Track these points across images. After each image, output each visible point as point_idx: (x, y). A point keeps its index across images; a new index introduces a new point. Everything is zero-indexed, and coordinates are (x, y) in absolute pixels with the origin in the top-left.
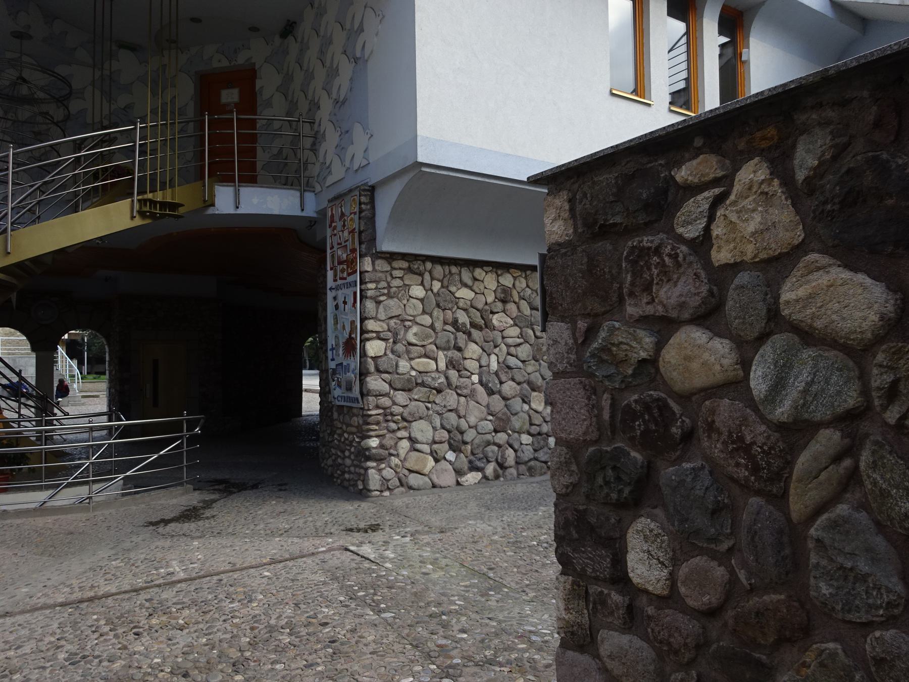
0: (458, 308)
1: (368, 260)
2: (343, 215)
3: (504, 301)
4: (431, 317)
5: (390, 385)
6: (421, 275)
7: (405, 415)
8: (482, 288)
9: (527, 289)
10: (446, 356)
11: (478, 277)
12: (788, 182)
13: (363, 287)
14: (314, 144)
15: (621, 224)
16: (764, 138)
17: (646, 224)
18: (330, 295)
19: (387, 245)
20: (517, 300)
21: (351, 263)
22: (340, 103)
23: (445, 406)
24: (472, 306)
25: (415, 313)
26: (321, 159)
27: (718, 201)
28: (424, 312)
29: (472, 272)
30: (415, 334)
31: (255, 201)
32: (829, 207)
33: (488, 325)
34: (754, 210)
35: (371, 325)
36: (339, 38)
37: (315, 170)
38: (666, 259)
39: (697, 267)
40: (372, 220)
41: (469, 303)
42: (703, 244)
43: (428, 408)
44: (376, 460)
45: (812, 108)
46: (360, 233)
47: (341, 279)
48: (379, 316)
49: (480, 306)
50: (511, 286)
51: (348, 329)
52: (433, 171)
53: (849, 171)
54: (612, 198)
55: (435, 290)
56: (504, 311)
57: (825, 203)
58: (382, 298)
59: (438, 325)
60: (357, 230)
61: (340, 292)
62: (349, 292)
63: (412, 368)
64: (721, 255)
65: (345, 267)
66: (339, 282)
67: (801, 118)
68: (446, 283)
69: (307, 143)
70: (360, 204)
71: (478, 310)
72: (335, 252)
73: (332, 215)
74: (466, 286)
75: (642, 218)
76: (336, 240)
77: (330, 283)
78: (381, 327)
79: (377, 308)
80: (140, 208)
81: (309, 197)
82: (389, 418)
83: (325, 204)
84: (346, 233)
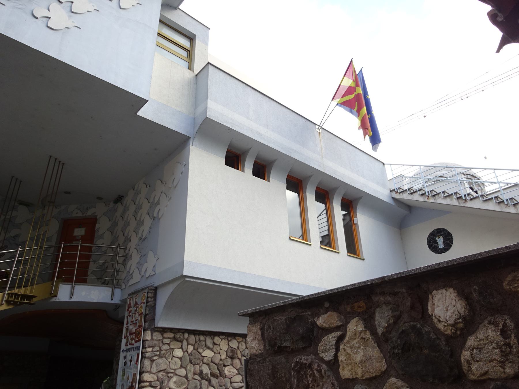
0: (203, 363)
1: (149, 332)
2: (136, 303)
3: (232, 358)
4: (186, 370)
6: (181, 341)
8: (218, 349)
9: (246, 350)
11: (216, 342)
12: (374, 333)
13: (144, 350)
14: (124, 261)
15: (290, 347)
16: (359, 307)
17: (303, 348)
18: (122, 355)
19: (161, 323)
20: (240, 357)
21: (137, 334)
22: (142, 240)
24: (212, 362)
25: (176, 368)
26: (127, 269)
27: (340, 339)
28: (182, 367)
29: (213, 339)
30: (175, 382)
31: (83, 293)
32: (396, 351)
33: (222, 374)
34: (359, 348)
35: (147, 377)
36: (146, 206)
37: (123, 276)
38: (315, 372)
39: (332, 378)
40: (153, 308)
41: (210, 359)
42: (334, 364)
45: (380, 294)
46: (146, 315)
47: (130, 344)
48: (152, 370)
49: (217, 361)
50: (236, 348)
51: (131, 379)
52: (192, 280)
53: (403, 332)
54: (284, 331)
55: (189, 352)
56: (232, 365)
57: (394, 348)
58: (155, 358)
59: (190, 376)
60: (144, 314)
61: (129, 354)
62: (134, 354)
64: (345, 373)
65: (134, 337)
66: (129, 346)
67: (375, 299)
68: (196, 347)
69: (121, 260)
70: (148, 297)
71: (216, 364)
72: (129, 327)
73: (130, 304)
74: (209, 348)
75: (301, 345)
76: (130, 319)
77: (123, 347)
78: (153, 378)
79: (152, 365)
80: (8, 298)
81: (117, 291)
83: (126, 296)
84: (137, 315)
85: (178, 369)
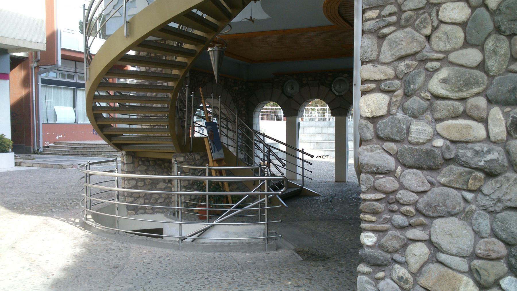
4: (482, 50)
5: (397, 159)
7: (420, 206)
10: (506, 115)
23: (499, 200)
25: (449, 47)
30: (444, 81)
43: (466, 200)
44: (369, 263)
48: (382, 58)
58: (385, 31)
63: (438, 135)
78: (384, 72)
79: (380, 46)
82: (395, 207)
85: (454, 50)
